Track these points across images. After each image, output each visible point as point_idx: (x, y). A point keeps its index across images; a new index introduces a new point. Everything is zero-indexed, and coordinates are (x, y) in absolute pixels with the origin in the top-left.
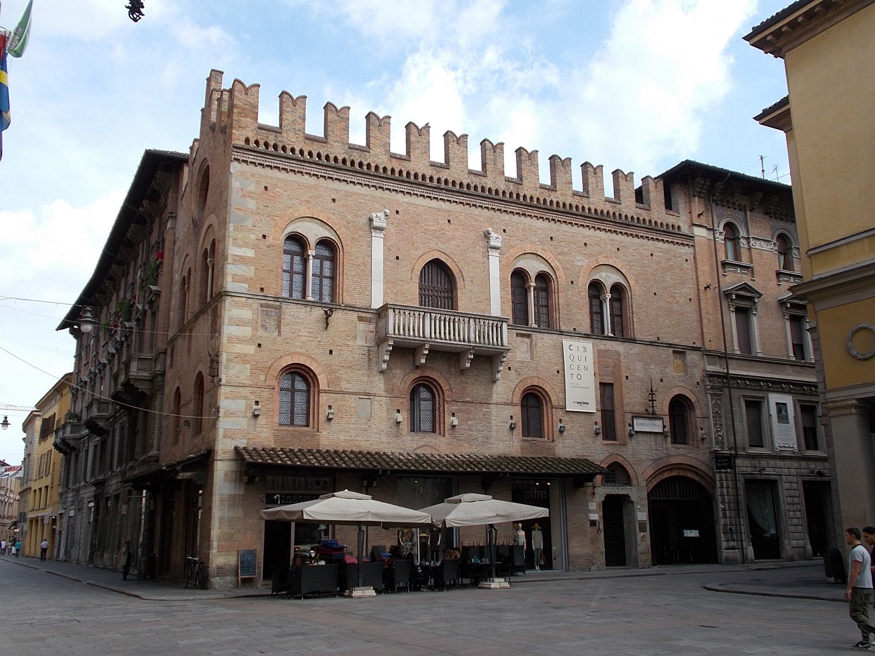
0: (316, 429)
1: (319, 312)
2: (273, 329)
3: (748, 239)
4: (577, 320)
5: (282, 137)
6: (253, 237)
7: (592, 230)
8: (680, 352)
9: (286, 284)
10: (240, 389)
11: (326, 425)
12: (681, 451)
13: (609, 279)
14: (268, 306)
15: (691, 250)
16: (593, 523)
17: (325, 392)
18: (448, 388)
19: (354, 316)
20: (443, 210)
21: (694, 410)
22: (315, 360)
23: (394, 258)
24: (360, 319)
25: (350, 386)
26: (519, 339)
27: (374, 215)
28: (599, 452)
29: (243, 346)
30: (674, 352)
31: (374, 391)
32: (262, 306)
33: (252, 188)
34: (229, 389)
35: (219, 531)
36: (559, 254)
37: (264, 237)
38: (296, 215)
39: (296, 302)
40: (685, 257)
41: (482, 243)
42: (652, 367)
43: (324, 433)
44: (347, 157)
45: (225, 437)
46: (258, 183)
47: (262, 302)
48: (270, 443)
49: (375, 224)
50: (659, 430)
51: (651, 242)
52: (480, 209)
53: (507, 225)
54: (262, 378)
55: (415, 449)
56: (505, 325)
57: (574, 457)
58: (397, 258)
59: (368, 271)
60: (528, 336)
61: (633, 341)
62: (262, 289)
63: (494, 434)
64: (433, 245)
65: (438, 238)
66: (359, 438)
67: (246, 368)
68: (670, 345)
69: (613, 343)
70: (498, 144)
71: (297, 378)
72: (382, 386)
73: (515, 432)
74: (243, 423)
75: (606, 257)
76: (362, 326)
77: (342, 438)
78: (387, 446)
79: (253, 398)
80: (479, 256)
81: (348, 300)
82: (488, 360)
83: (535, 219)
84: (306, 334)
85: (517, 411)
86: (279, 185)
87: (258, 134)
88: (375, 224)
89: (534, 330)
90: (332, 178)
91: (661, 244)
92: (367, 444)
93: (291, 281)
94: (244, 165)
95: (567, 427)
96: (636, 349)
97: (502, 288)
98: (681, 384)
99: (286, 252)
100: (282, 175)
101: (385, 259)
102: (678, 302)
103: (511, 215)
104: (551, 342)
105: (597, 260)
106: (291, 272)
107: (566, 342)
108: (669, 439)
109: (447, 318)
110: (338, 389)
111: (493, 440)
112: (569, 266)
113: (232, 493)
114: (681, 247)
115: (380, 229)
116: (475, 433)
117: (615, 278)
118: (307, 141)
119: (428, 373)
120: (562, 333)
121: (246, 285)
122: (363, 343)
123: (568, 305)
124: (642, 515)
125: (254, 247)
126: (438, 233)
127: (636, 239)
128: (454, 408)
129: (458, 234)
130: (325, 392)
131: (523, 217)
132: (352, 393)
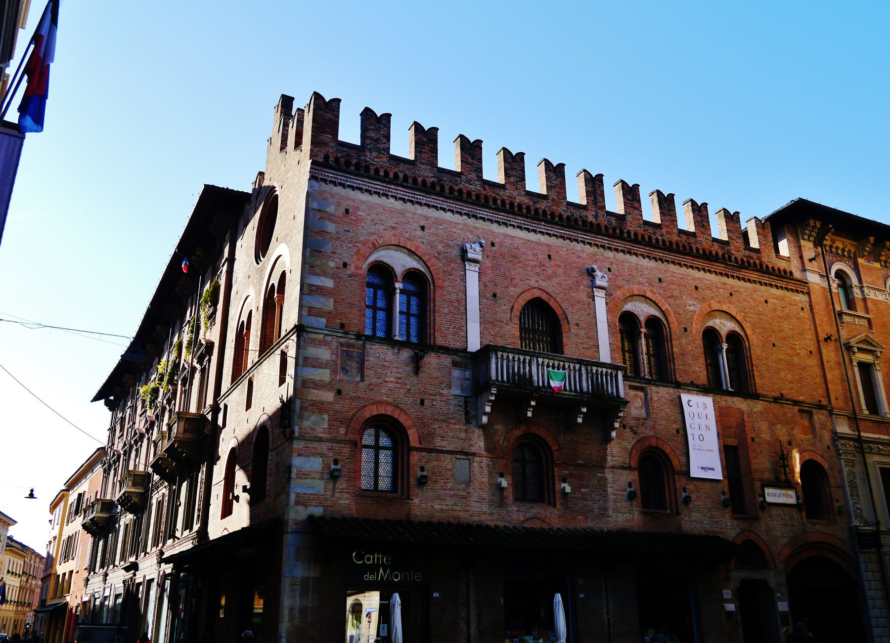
0: (405, 496)
1: (406, 354)
2: (355, 372)
3: (861, 288)
4: (694, 372)
5: (365, 156)
6: (332, 264)
7: (702, 272)
8: (806, 410)
9: (368, 322)
10: (316, 444)
11: (417, 491)
12: (818, 527)
13: (724, 326)
14: (349, 346)
15: (805, 298)
16: (730, 613)
19: (447, 360)
20: (542, 244)
21: (828, 478)
23: (490, 296)
24: (455, 364)
25: (445, 443)
27: (468, 246)
28: (728, 527)
29: (320, 392)
30: (800, 411)
31: (473, 450)
32: (342, 345)
34: (302, 444)
35: (288, 624)
36: (669, 297)
37: (345, 265)
39: (382, 341)
40: (800, 305)
41: (586, 281)
42: (779, 427)
43: (416, 501)
45: (297, 503)
46: (338, 204)
47: (341, 340)
49: (470, 255)
50: (792, 501)
51: (763, 288)
52: (581, 244)
53: (612, 264)
54: (342, 431)
55: (523, 522)
56: (620, 375)
58: (495, 295)
59: (462, 308)
60: (642, 389)
61: (756, 396)
62: (342, 326)
63: (611, 504)
64: (533, 283)
65: (538, 274)
67: (323, 419)
68: (796, 403)
69: (735, 399)
70: (597, 176)
71: (382, 434)
72: (482, 444)
74: (319, 486)
75: (718, 302)
76: (456, 373)
77: (437, 507)
78: (489, 518)
80: (583, 296)
81: (440, 341)
83: (640, 257)
84: (393, 379)
85: (634, 476)
86: (362, 207)
88: (470, 255)
89: (649, 382)
91: (774, 291)
92: (467, 515)
93: (374, 318)
94: (323, 184)
95: (693, 497)
96: (759, 406)
97: (611, 333)
98: (810, 448)
99: (369, 285)
100: (365, 197)
102: (798, 354)
103: (615, 252)
104: (667, 396)
105: (710, 306)
106: (374, 308)
107: (685, 397)
108: (804, 514)
111: (610, 512)
113: (306, 575)
114: (795, 294)
115: (475, 261)
117: (730, 326)
118: (392, 162)
119: (534, 430)
120: (678, 385)
121: (324, 320)
122: (458, 392)
123: (683, 355)
124: (783, 606)
125: (334, 276)
126: (538, 270)
127: (748, 285)
129: (560, 271)
131: (628, 256)
132: (447, 452)
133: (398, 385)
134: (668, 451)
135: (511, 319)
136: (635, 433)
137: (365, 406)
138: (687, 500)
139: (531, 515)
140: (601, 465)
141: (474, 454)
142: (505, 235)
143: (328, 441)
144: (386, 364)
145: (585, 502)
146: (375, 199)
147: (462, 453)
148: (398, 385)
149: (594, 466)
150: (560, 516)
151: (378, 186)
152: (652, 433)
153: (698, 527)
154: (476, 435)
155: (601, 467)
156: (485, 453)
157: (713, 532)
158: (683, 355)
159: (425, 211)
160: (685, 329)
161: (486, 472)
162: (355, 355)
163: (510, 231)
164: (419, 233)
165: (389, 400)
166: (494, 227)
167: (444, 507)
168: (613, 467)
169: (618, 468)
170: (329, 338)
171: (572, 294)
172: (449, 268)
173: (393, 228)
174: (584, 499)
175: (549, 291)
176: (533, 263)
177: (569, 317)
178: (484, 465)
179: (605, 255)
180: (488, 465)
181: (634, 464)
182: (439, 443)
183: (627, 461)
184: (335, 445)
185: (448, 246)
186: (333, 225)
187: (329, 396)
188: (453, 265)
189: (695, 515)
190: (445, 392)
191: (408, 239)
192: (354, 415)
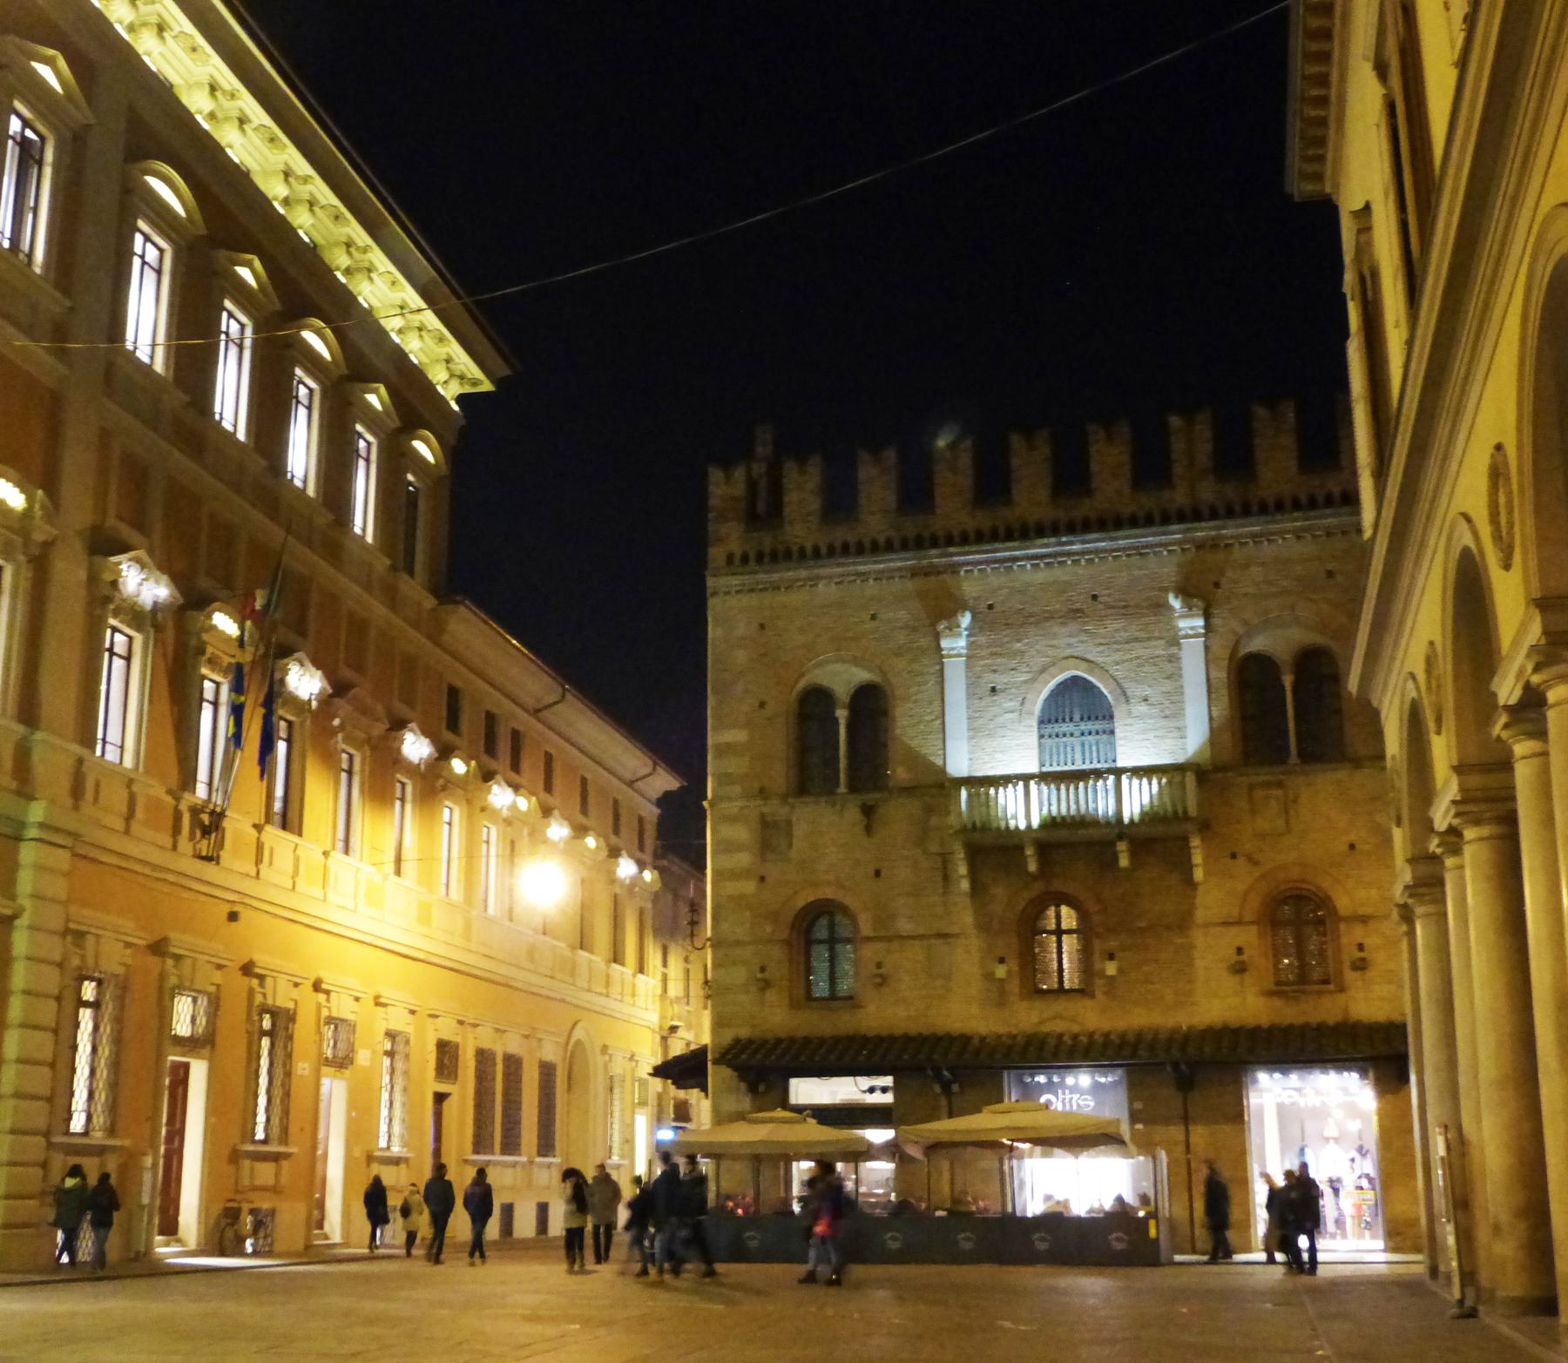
17: (869, 939)
18: (1097, 908)
43: (872, 1008)
54: (769, 929)
60: (1280, 785)
128: (1113, 944)
130: (869, 939)
136: (1256, 863)
138: (1361, 965)
140: (1184, 923)
141: (956, 936)
149: (1168, 927)
168: (1207, 925)
169: (1218, 924)
189: (1381, 990)
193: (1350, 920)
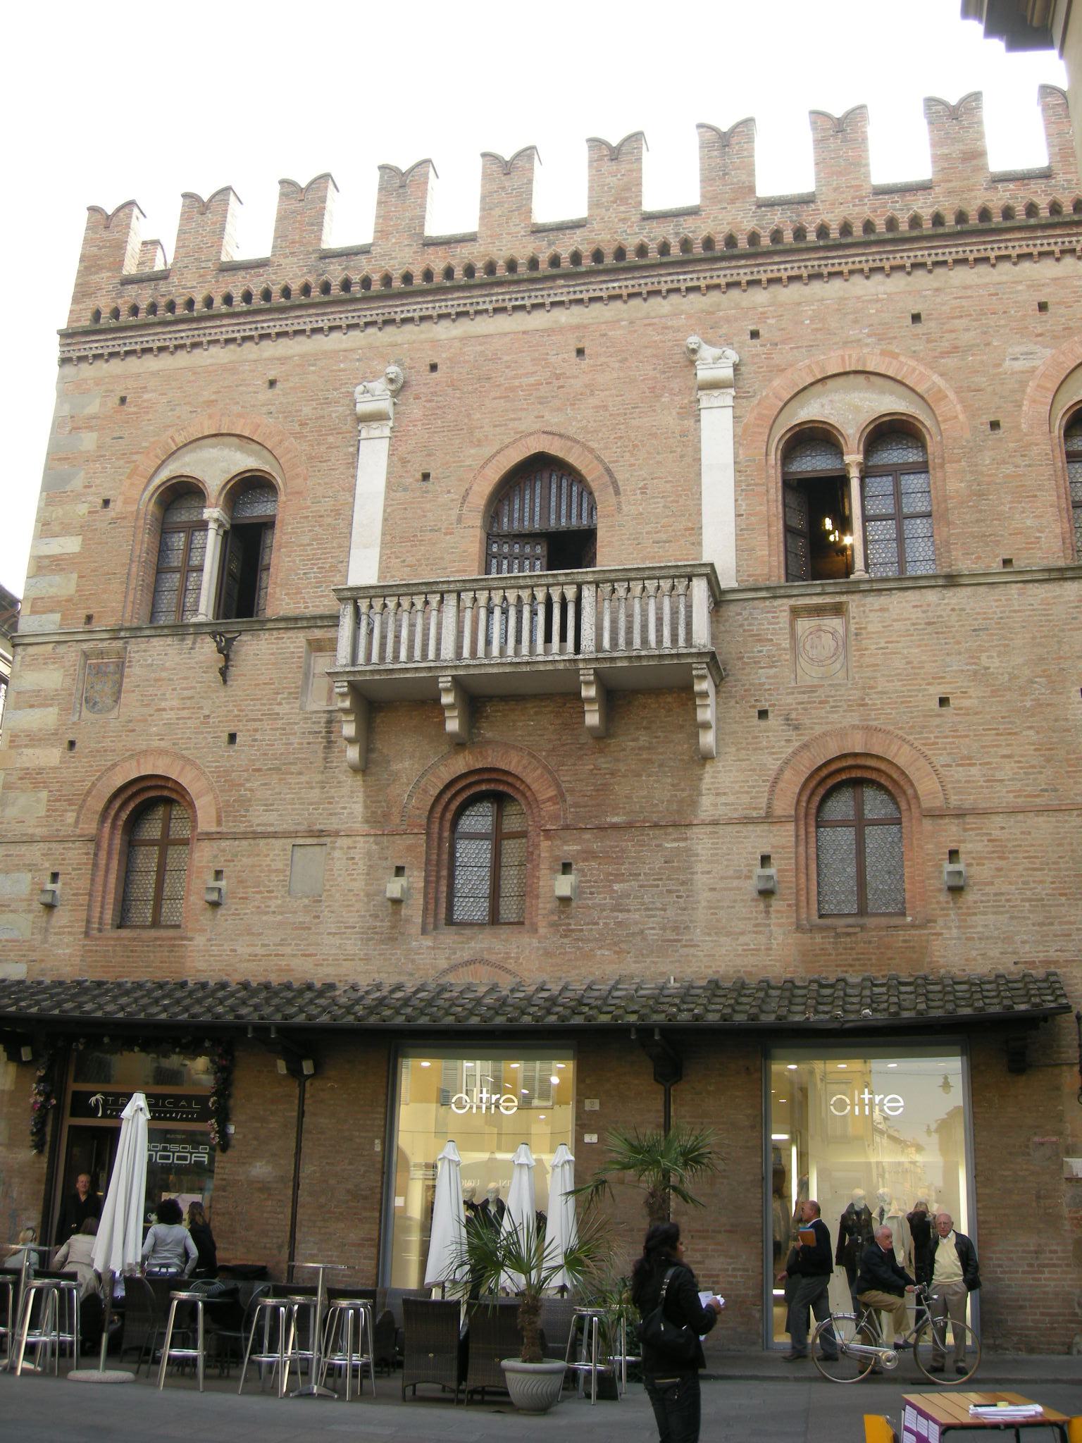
6: (83, 509)
10: (24, 849)
11: (205, 918)
14: (101, 654)
17: (209, 836)
18: (552, 792)
20: (561, 330)
22: (193, 764)
23: (413, 478)
25: (272, 817)
26: (804, 625)
29: (38, 751)
31: (333, 824)
32: (86, 655)
33: (93, 408)
38: (181, 440)
43: (200, 940)
44: (311, 279)
47: (85, 646)
48: (69, 972)
53: (763, 317)
54: (70, 817)
57: (1006, 965)
64: (528, 423)
65: (542, 401)
66: (288, 950)
67: (38, 801)
72: (358, 808)
73: (777, 904)
77: (243, 950)
79: (48, 866)
80: (669, 420)
82: (648, 695)
84: (175, 703)
85: (781, 839)
87: (120, 295)
88: (361, 408)
90: (268, 336)
100: (151, 363)
101: (392, 486)
109: (511, 596)
110: (242, 828)
111: (697, 935)
112: (981, 380)
116: (637, 916)
121: (57, 617)
125: (84, 530)
128: (570, 849)
130: (209, 836)
131: (816, 286)
132: (275, 835)
133: (185, 713)
134: (900, 761)
135: (459, 520)
137: (115, 765)
139: (466, 955)
141: (336, 834)
142: (464, 339)
143: (44, 840)
144: (164, 674)
145: (621, 916)
146: (182, 359)
147: (312, 833)
148: (185, 713)
149: (656, 826)
150: (547, 954)
151: (185, 334)
152: (854, 719)
153: (994, 953)
154: (345, 790)
155: (675, 825)
156: (366, 828)
157: (1047, 962)
158: (981, 495)
159: (270, 349)
160: (995, 425)
161: (362, 866)
162: (112, 668)
163: (483, 326)
164: (266, 395)
165: (162, 744)
166: (444, 331)
167: (260, 951)
168: (715, 823)
170: (62, 649)
171: (635, 423)
172: (323, 448)
173: (211, 403)
174: (618, 908)
175: (571, 431)
176: (532, 380)
177: (619, 476)
178: (358, 854)
179: (744, 304)
180: (369, 854)
181: (784, 805)
182: (260, 818)
183: (763, 802)
184: (54, 845)
185: (327, 402)
186: (95, 435)
187: (51, 756)
188: (331, 439)
190: (283, 709)
191: (240, 415)
192: (94, 785)
193: (936, 815)
